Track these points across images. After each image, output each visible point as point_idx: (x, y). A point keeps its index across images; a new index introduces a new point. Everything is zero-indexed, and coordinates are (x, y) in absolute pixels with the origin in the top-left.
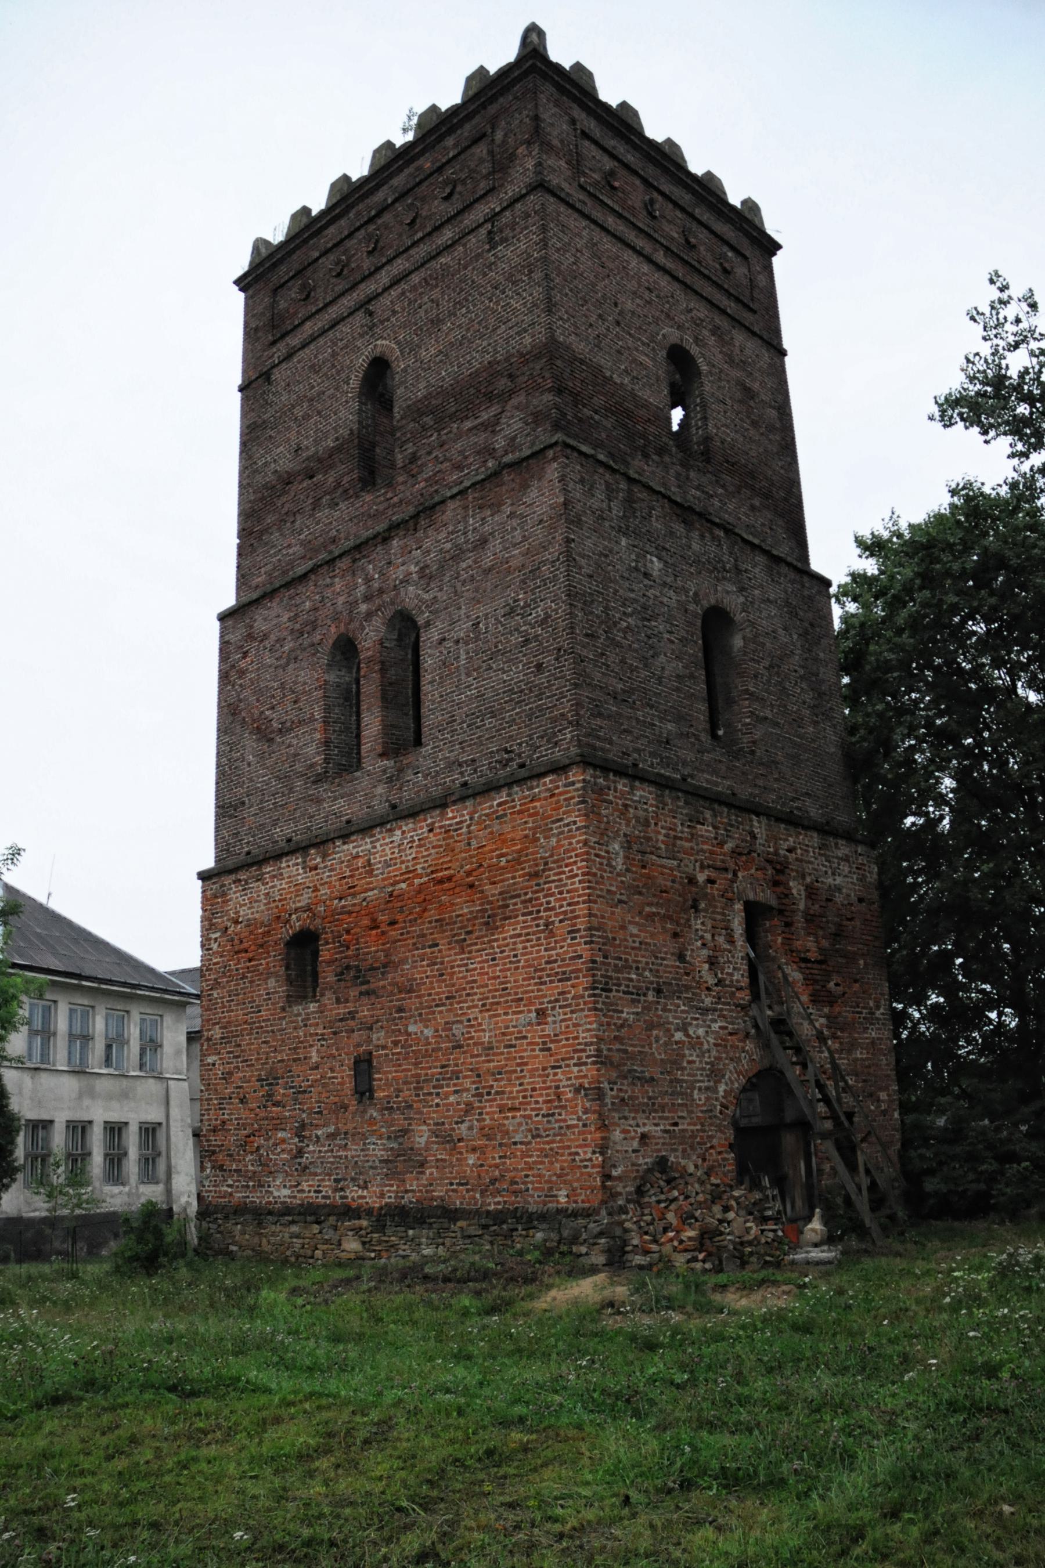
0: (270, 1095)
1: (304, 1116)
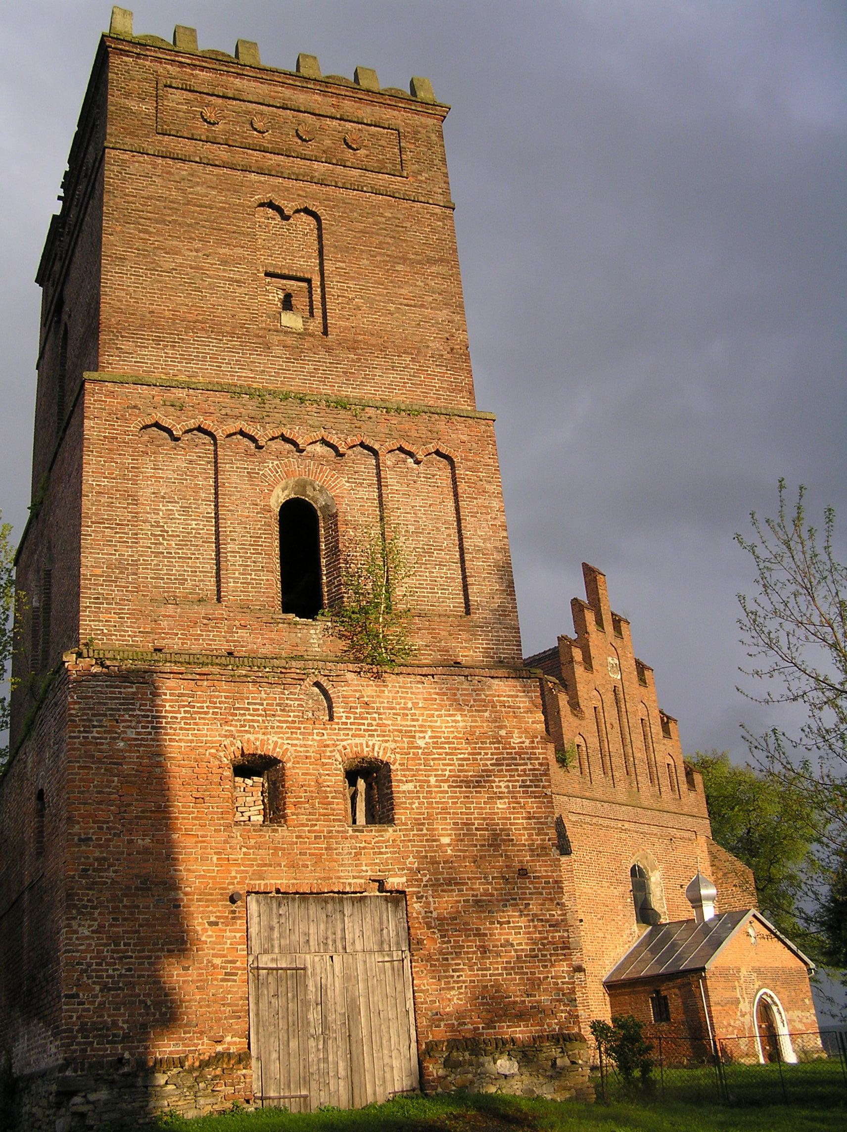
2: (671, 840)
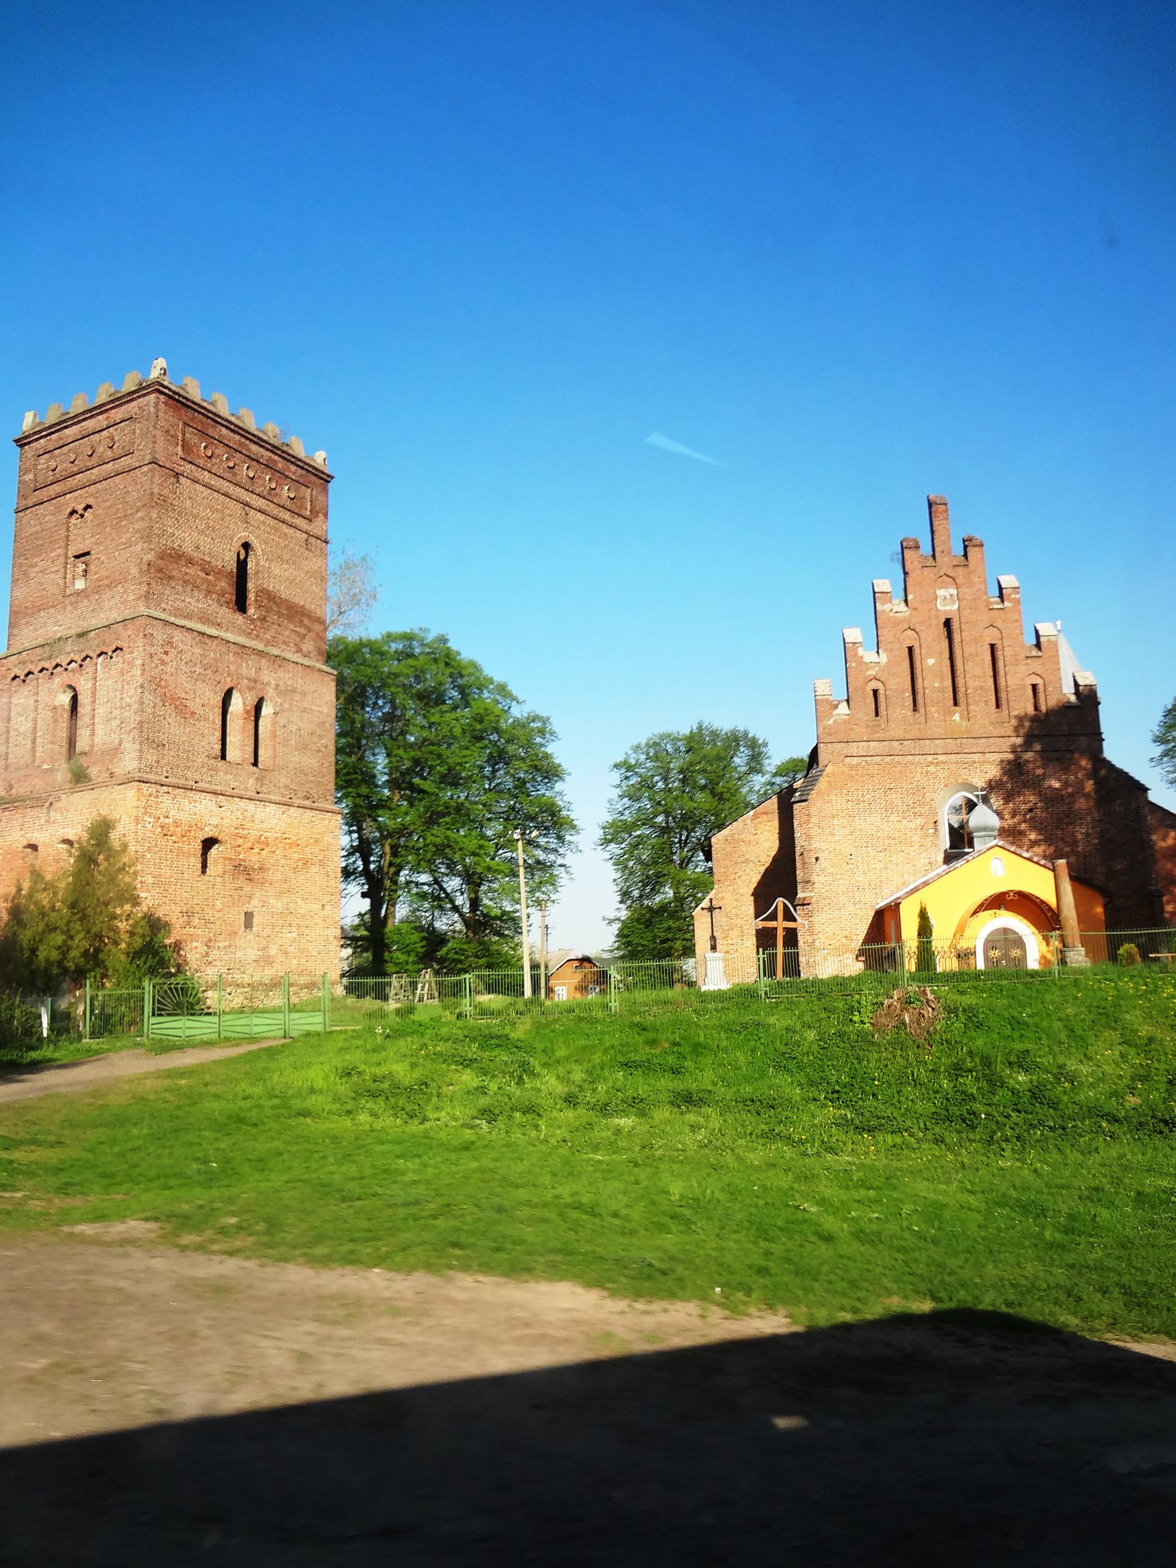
0: (189, 923)
1: (211, 935)
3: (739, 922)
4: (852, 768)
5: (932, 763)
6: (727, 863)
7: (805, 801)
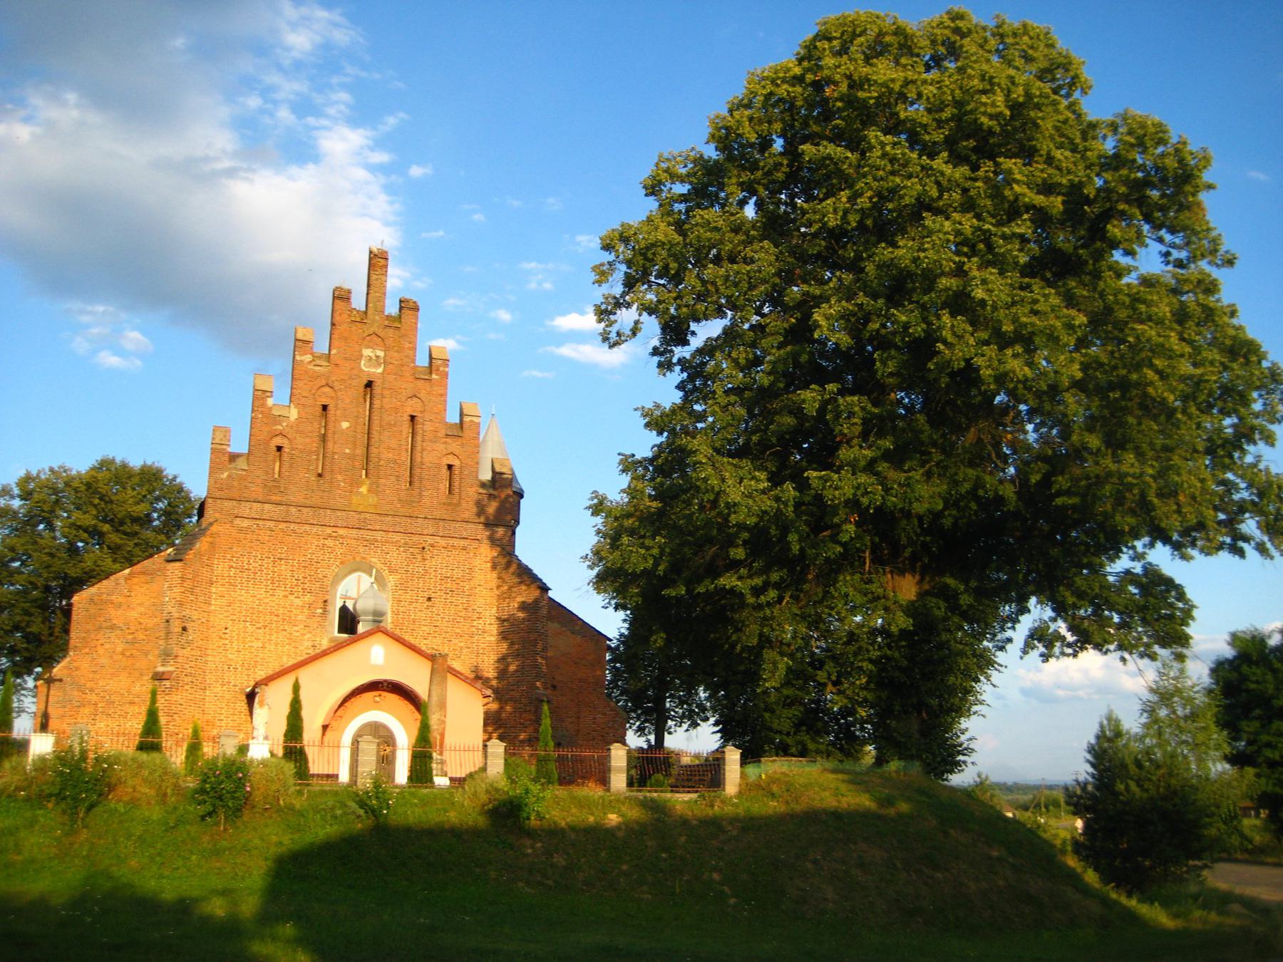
2: (424, 548)
3: (94, 698)
4: (241, 530)
5: (330, 536)
6: (89, 627)
7: (181, 560)
